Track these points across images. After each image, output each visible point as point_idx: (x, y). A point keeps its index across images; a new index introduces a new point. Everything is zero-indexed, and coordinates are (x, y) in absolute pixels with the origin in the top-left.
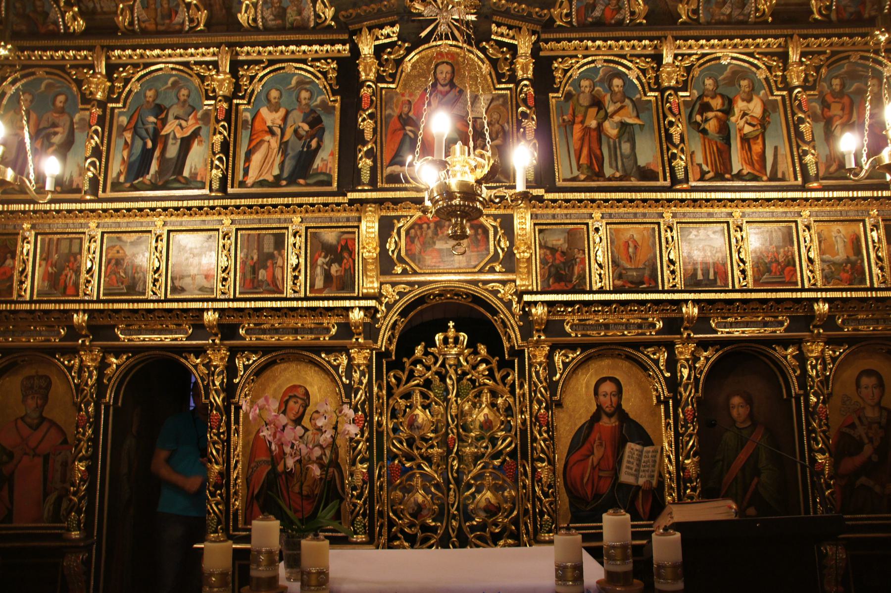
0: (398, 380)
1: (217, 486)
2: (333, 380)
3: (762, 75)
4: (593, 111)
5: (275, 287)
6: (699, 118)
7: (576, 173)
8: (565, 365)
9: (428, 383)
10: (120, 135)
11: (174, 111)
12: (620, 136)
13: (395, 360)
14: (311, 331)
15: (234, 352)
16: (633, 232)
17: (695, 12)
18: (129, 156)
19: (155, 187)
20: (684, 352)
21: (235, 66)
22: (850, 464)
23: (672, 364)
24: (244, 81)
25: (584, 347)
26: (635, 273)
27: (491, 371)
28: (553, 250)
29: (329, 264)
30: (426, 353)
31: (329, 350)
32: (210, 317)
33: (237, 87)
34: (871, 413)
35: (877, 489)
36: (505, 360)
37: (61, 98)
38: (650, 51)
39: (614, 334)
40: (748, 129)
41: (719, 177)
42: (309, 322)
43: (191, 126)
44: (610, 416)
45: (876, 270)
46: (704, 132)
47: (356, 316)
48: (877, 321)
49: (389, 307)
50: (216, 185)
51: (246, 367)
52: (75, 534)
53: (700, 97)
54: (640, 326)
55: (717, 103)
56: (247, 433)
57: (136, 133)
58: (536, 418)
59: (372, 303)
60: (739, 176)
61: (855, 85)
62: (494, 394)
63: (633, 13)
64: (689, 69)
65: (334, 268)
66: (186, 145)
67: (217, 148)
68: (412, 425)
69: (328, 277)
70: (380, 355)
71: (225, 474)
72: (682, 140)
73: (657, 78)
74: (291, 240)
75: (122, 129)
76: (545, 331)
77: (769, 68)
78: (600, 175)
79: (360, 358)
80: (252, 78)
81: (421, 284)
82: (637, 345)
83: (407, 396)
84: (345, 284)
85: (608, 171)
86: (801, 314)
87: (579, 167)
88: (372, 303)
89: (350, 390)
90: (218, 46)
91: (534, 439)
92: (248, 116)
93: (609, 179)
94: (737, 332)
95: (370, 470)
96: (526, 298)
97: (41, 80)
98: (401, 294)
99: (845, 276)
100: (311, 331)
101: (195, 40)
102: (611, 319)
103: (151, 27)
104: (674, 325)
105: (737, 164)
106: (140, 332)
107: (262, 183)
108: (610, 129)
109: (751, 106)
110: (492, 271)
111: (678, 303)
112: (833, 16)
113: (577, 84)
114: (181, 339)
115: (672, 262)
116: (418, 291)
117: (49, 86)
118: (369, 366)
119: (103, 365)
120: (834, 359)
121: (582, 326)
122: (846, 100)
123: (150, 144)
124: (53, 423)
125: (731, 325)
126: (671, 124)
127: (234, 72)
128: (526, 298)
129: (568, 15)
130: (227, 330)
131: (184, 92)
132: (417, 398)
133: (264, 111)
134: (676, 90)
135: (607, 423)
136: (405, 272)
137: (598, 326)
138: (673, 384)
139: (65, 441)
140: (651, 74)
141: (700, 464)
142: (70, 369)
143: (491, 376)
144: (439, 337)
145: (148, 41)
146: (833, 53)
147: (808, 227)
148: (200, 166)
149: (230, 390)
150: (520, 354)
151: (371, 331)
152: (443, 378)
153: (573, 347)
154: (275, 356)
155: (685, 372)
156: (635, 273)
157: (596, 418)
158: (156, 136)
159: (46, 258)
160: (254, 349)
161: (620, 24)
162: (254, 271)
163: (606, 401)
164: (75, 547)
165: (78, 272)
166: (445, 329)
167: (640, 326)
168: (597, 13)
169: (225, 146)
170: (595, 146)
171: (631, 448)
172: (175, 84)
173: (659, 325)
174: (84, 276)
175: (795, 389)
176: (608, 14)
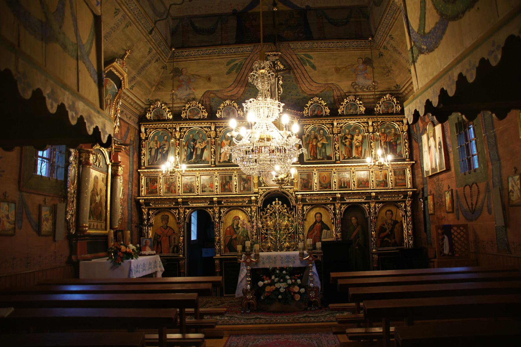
0: (263, 214)
1: (218, 242)
2: (246, 214)
3: (362, 128)
4: (315, 140)
5: (230, 190)
6: (344, 141)
7: (310, 158)
8: (307, 210)
9: (271, 214)
10: (184, 148)
11: (198, 141)
12: (322, 147)
13: (262, 209)
14: (241, 202)
15: (220, 208)
16: (325, 174)
17: (343, 111)
18: (187, 153)
19: (195, 163)
20: (338, 206)
21: (216, 128)
22: (383, 235)
23: (335, 209)
24: (218, 133)
25: (312, 205)
26: (326, 185)
27: (287, 211)
28: (303, 179)
29: (244, 184)
30: (270, 207)
31: (246, 207)
32: (215, 199)
33: (216, 134)
34: (389, 221)
35: (390, 241)
36: (291, 208)
37: (166, 137)
38: (330, 122)
39: (319, 202)
40: (357, 144)
41: (349, 158)
42: (240, 200)
43: (203, 145)
44: (319, 223)
45: (390, 183)
46: (345, 145)
47: (253, 198)
48: (389, 197)
49: (261, 195)
50: (213, 163)
51: (224, 212)
52: (181, 256)
53: (345, 135)
54: (326, 199)
55: (349, 137)
56: (224, 229)
57: (188, 147)
58: (299, 223)
59: (257, 195)
60: (355, 158)
61: (388, 130)
62: (289, 217)
63: (326, 112)
64: (341, 127)
65: (246, 185)
66: (203, 150)
67: (213, 153)
68: (267, 226)
69: (244, 188)
70: (258, 208)
71: (219, 239)
72: (338, 148)
73: (332, 130)
74: (234, 178)
75: (184, 146)
76: (301, 201)
77: (364, 127)
78: (316, 158)
79: (254, 209)
80: (220, 132)
81: (269, 189)
82: (325, 204)
83: (266, 218)
84: (249, 189)
85: (319, 157)
86: (368, 196)
87: (311, 156)
88: (257, 195)
89: (251, 217)
90: (211, 123)
91: (299, 229)
92: (220, 142)
93: (319, 159)
94: (352, 201)
95: (257, 237)
96: (296, 193)
97: (160, 132)
98: (264, 192)
99: (382, 185)
100: (241, 202)
101: (205, 121)
102: (318, 198)
103: (192, 117)
104: (335, 199)
105: (354, 154)
106: (195, 203)
107: (225, 162)
108: (319, 145)
109: (359, 137)
110: (287, 185)
111: (336, 193)
112: (381, 112)
113: (310, 132)
114: (206, 205)
115: (335, 182)
116: (268, 191)
117: (162, 133)
118: (256, 211)
119: (185, 212)
120: (378, 207)
121: (311, 200)
122: (385, 135)
123: (192, 150)
124: (171, 228)
125: (350, 199)
126: (336, 144)
127: (215, 130)
128: (296, 193)
129: (308, 113)
130: (219, 202)
131: (201, 135)
132: (268, 218)
133: (224, 141)
134: (337, 134)
135: (318, 224)
136: (265, 186)
137: (315, 200)
138: (335, 214)
139: (174, 232)
140: (331, 129)
141: (341, 235)
142: (175, 213)
143: (288, 212)
144: (274, 203)
145: (191, 122)
146: (382, 122)
147: (372, 172)
148: (207, 157)
149: (220, 218)
150: (295, 207)
151: (256, 202)
152: (275, 213)
153: (309, 205)
154: (231, 208)
155: (338, 211)
156: (326, 185)
157: (315, 223)
158: (194, 148)
159: (166, 183)
160: (226, 207)
161: (322, 116)
162: (224, 186)
163: (318, 219)
164: (182, 259)
165: (175, 187)
166: (275, 200)
167: (326, 199)
168: (316, 113)
169: (215, 151)
170: (315, 150)
171: (324, 231)
172: (198, 132)
173: (331, 199)
174: (177, 188)
175: (368, 215)
176: (319, 113)
